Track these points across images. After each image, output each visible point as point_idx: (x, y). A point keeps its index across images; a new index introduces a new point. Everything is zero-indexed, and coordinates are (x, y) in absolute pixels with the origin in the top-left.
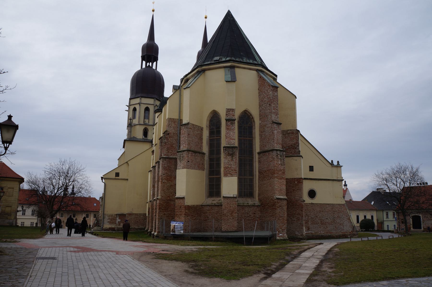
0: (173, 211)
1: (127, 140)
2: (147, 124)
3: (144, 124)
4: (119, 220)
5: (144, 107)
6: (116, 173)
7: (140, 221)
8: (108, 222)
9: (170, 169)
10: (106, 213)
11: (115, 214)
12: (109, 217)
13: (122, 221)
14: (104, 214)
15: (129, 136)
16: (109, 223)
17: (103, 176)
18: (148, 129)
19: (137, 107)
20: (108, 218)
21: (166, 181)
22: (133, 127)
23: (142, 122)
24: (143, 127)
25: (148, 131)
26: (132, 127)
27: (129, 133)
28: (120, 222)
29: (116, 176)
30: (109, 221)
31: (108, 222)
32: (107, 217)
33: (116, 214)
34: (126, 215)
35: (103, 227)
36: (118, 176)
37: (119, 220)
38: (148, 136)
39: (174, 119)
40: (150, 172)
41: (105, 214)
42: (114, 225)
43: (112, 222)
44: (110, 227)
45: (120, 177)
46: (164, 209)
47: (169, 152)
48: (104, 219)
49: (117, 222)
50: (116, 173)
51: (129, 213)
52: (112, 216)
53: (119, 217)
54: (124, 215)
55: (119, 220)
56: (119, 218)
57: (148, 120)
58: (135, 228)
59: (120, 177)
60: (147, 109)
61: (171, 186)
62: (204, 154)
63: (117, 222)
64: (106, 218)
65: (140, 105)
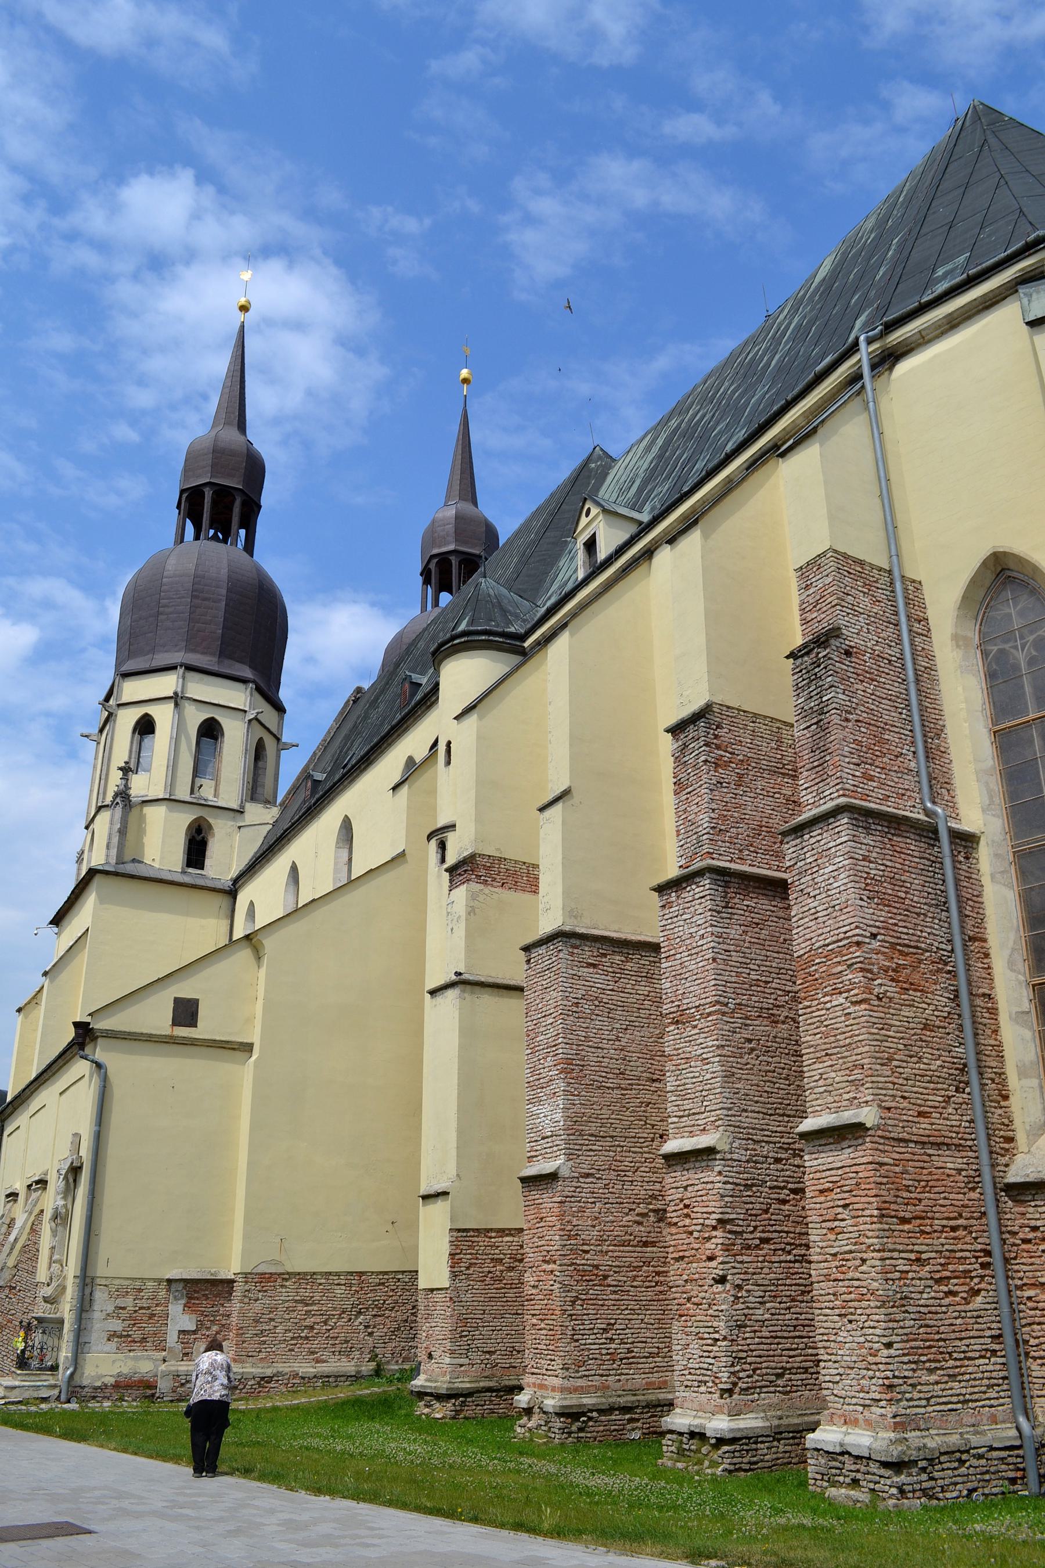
0: (965, 1228)
1: (107, 868)
2: (210, 803)
3: (195, 801)
4: (188, 1322)
5: (195, 717)
6: (177, 1001)
7: (325, 1323)
8: (112, 1336)
9: (903, 895)
10: (101, 1270)
11: (160, 1281)
12: (120, 1302)
13: (208, 1329)
14: (88, 1280)
15: (114, 852)
16: (113, 1345)
17: (88, 1019)
18: (210, 827)
19: (163, 716)
20: (110, 1308)
21: (892, 989)
22: (135, 811)
23: (183, 792)
24: (185, 819)
25: (213, 836)
26: (131, 807)
27: (115, 840)
28: (194, 1332)
29: (176, 1022)
30: (117, 1325)
31: (112, 1336)
32: (103, 1302)
33: (170, 1281)
34: (232, 1281)
35: (72, 1375)
36: (193, 1024)
37: (188, 1322)
38: (207, 862)
39: (861, 563)
40: (452, 994)
41: (93, 1279)
42: (149, 1358)
43: (137, 1335)
44: (119, 1375)
45: (201, 1031)
46: (908, 1215)
47: (871, 778)
48: (84, 1315)
49: (172, 1338)
50: (177, 1001)
51: (263, 1269)
52: (140, 1290)
53: (183, 1302)
54: (222, 1281)
55: (186, 1317)
56: (185, 1306)
57: (213, 783)
58: (296, 1375)
59: (205, 1029)
60: (210, 731)
61: (926, 1027)
62: (965, 841)
63: (172, 1338)
64: (96, 1307)
65: (176, 705)
